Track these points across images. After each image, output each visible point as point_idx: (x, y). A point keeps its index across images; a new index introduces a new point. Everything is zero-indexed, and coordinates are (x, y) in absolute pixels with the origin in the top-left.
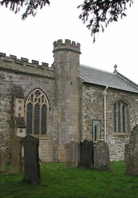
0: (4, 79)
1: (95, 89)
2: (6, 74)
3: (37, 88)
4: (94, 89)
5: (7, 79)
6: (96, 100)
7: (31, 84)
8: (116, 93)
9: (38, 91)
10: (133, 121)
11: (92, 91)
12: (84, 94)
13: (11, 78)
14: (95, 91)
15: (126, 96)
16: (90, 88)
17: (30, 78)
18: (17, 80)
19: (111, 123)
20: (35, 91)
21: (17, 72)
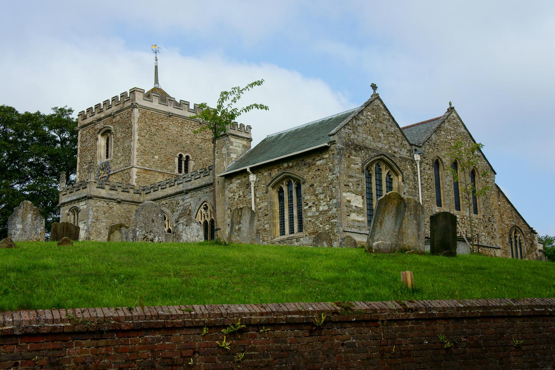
0: (179, 204)
1: (240, 179)
2: (179, 198)
3: (205, 202)
4: (238, 179)
5: (181, 203)
6: (241, 194)
7: (200, 199)
8: (275, 169)
9: (206, 205)
10: (310, 207)
11: (235, 183)
12: (227, 192)
13: (183, 200)
14: (239, 181)
15: (295, 166)
16: (234, 180)
17: (199, 192)
18: (188, 200)
19: (266, 222)
20: (202, 206)
21: (187, 192)
